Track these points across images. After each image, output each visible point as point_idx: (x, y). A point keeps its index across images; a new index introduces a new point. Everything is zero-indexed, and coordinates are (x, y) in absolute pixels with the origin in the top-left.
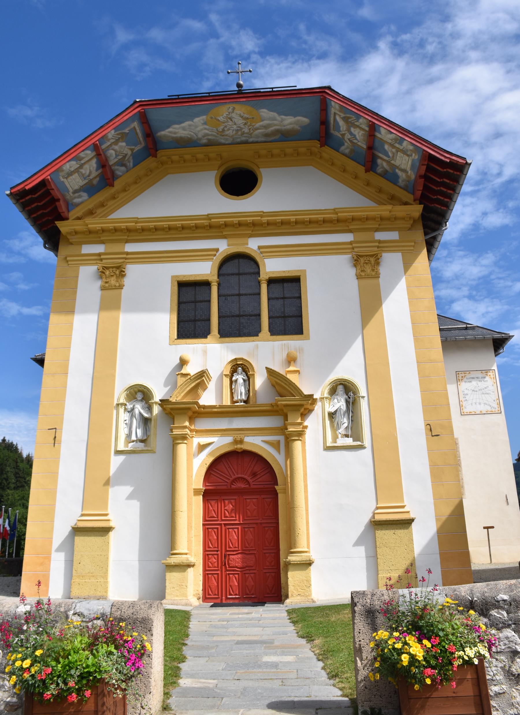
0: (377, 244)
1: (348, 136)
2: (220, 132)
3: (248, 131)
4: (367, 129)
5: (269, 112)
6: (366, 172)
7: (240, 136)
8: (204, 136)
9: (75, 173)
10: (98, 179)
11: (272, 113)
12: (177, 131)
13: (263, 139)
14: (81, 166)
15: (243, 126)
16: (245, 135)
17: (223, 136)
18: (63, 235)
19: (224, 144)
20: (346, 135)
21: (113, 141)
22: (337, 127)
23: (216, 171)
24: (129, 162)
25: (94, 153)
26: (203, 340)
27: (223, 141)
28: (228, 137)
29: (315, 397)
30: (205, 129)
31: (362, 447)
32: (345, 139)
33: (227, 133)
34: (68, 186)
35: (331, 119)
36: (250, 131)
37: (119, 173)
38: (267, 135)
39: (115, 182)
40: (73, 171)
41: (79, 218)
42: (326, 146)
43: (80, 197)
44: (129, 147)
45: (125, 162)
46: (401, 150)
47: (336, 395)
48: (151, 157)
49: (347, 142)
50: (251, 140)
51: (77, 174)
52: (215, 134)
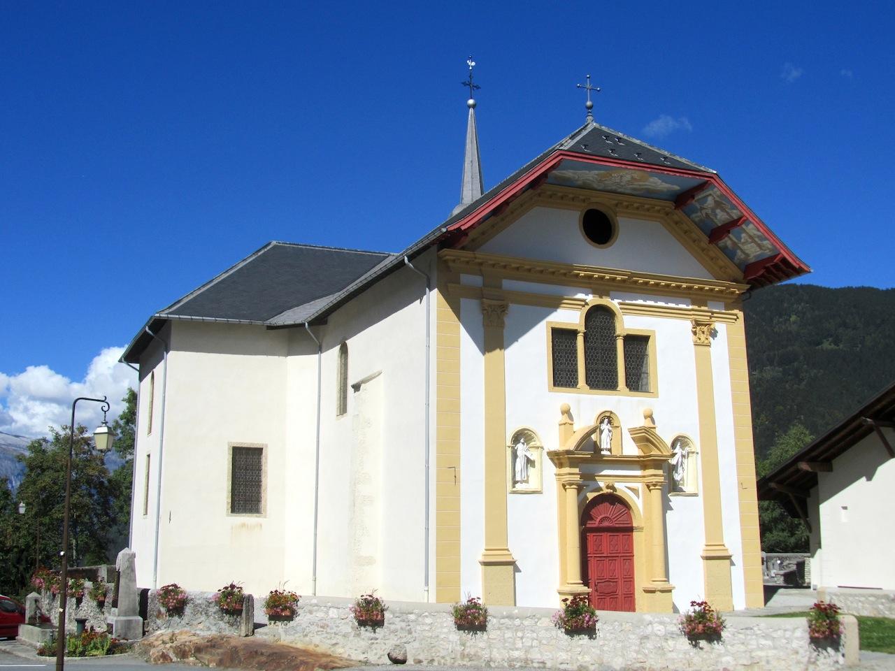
0: (710, 314)
19: (596, 190)
31: (695, 495)
42: (680, 210)
50: (619, 190)
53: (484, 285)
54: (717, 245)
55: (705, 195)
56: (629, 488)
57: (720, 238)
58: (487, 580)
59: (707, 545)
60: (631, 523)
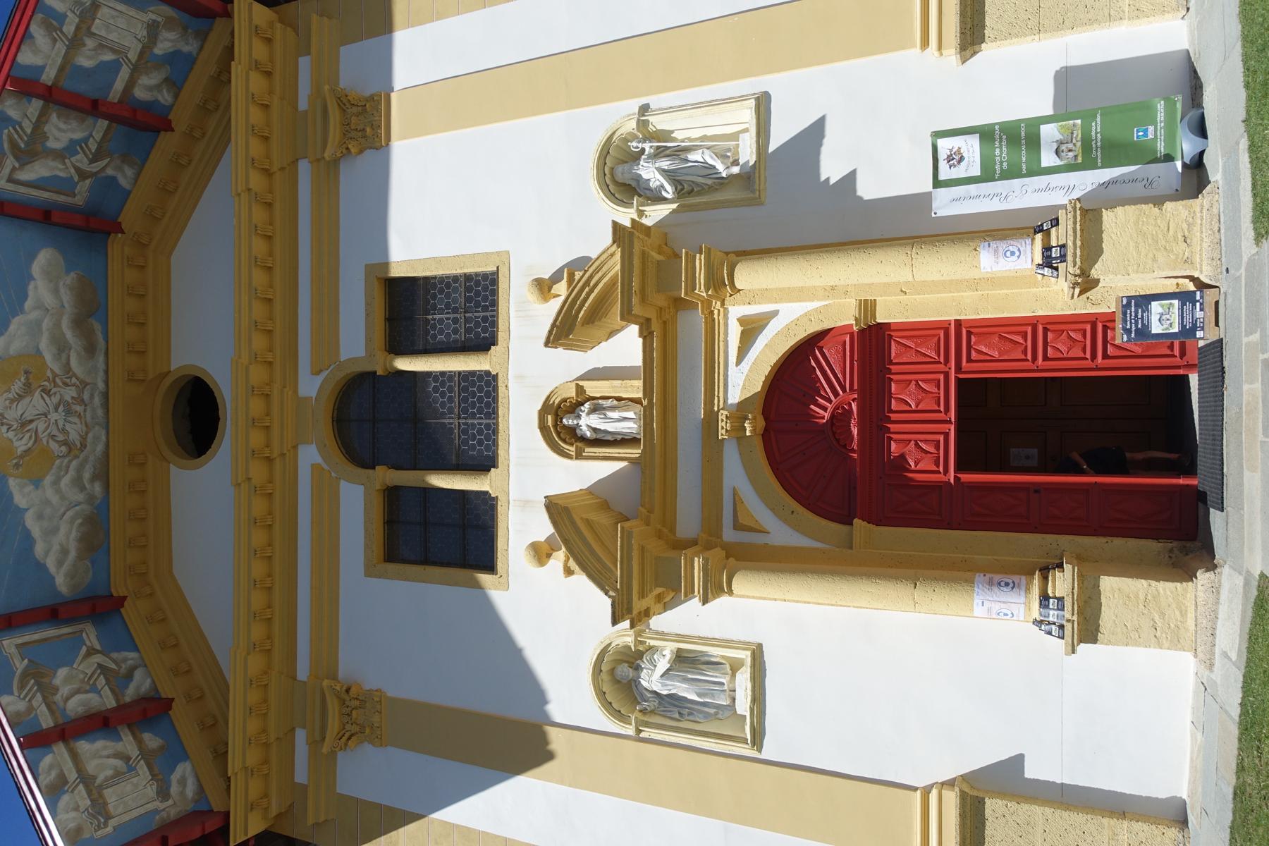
1: (77, 161)
2: (70, 450)
3: (74, 388)
4: (36, 105)
5: (8, 333)
6: (173, 130)
7: (88, 408)
8: (83, 489)
9: (101, 796)
10: (147, 736)
11: (12, 327)
12: (56, 547)
13: (101, 359)
14: (86, 779)
15: (56, 399)
16: (86, 396)
17: (83, 446)
18: (272, 826)
20: (78, 164)
21: (39, 697)
22: (61, 185)
23: (171, 465)
24: (125, 660)
25: (60, 749)
26: (501, 509)
27: (100, 448)
28: (90, 435)
29: (628, 224)
30: (56, 482)
32: (94, 170)
33: (74, 436)
34: (135, 814)
35: (33, 194)
36: (74, 385)
37: (147, 685)
38: (90, 349)
39: (163, 696)
40: (91, 800)
43: (183, 782)
44: (80, 658)
45: (123, 671)
46: (81, 21)
47: (638, 185)
48: (122, 610)
49: (103, 169)
50: (101, 385)
51: (108, 793)
52: (74, 463)
53: (304, 728)
54: (172, 106)
55: (35, 193)
56: (740, 360)
57: (149, 106)
59: (925, 43)
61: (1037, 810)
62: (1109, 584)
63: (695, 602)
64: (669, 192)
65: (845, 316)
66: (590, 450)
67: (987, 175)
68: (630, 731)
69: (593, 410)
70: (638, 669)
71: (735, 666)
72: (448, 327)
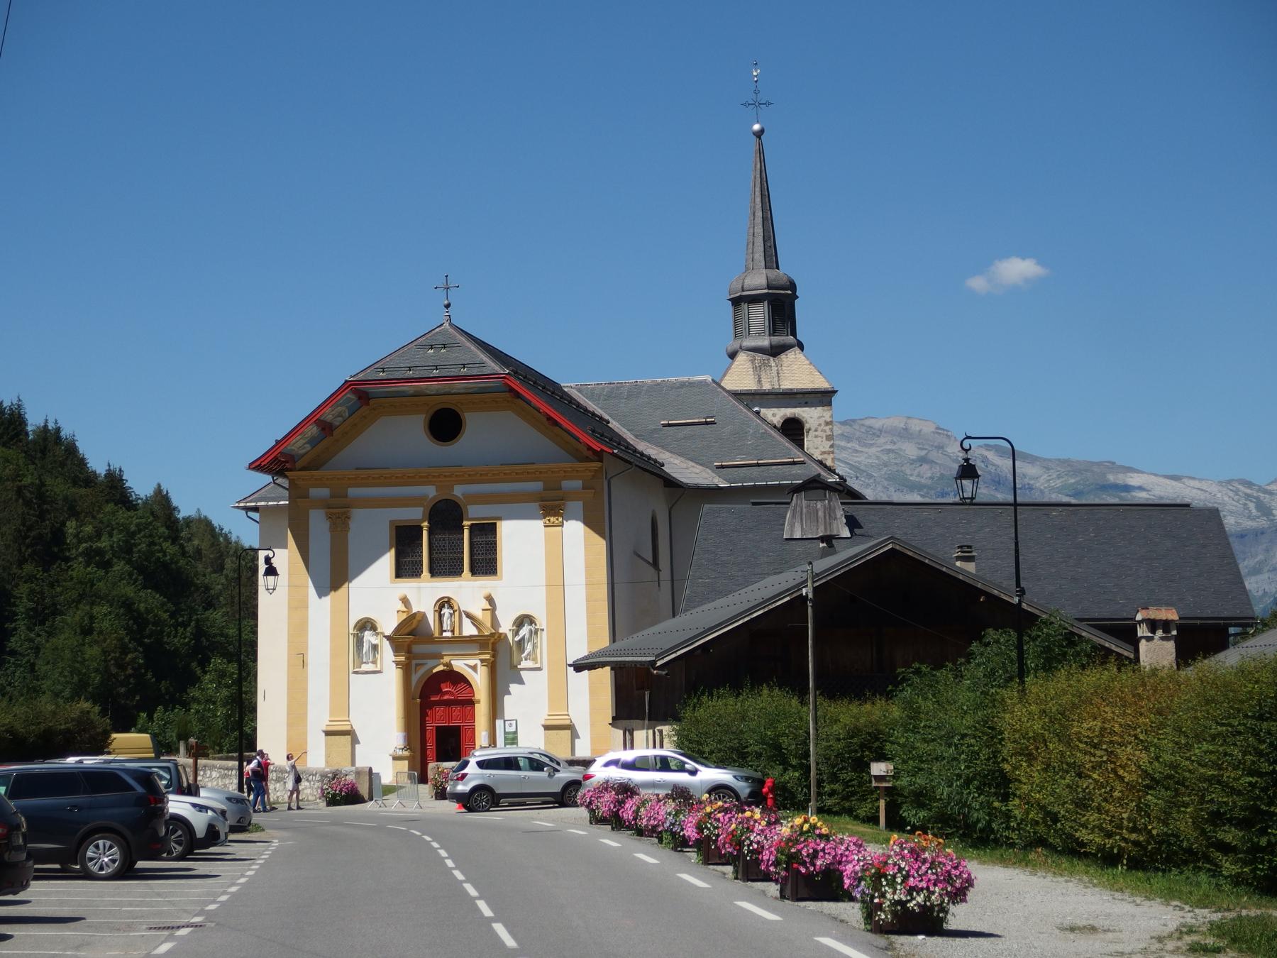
31: (539, 669)
41: (303, 469)
50: (453, 391)
56: (465, 664)
58: (328, 747)
60: (474, 696)
61: (350, 748)
62: (406, 762)
63: (394, 659)
64: (517, 639)
65: (477, 696)
66: (437, 614)
67: (505, 733)
68: (351, 631)
69: (451, 615)
70: (370, 630)
71: (374, 662)
72: (481, 551)
